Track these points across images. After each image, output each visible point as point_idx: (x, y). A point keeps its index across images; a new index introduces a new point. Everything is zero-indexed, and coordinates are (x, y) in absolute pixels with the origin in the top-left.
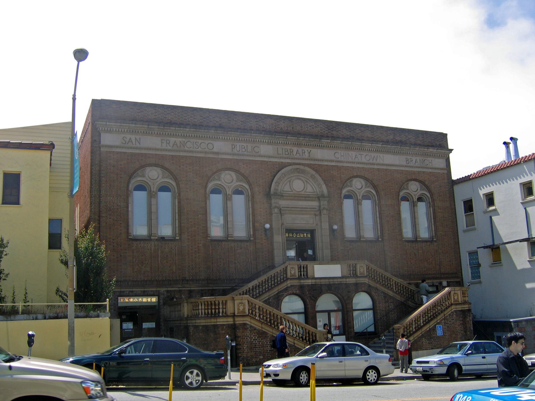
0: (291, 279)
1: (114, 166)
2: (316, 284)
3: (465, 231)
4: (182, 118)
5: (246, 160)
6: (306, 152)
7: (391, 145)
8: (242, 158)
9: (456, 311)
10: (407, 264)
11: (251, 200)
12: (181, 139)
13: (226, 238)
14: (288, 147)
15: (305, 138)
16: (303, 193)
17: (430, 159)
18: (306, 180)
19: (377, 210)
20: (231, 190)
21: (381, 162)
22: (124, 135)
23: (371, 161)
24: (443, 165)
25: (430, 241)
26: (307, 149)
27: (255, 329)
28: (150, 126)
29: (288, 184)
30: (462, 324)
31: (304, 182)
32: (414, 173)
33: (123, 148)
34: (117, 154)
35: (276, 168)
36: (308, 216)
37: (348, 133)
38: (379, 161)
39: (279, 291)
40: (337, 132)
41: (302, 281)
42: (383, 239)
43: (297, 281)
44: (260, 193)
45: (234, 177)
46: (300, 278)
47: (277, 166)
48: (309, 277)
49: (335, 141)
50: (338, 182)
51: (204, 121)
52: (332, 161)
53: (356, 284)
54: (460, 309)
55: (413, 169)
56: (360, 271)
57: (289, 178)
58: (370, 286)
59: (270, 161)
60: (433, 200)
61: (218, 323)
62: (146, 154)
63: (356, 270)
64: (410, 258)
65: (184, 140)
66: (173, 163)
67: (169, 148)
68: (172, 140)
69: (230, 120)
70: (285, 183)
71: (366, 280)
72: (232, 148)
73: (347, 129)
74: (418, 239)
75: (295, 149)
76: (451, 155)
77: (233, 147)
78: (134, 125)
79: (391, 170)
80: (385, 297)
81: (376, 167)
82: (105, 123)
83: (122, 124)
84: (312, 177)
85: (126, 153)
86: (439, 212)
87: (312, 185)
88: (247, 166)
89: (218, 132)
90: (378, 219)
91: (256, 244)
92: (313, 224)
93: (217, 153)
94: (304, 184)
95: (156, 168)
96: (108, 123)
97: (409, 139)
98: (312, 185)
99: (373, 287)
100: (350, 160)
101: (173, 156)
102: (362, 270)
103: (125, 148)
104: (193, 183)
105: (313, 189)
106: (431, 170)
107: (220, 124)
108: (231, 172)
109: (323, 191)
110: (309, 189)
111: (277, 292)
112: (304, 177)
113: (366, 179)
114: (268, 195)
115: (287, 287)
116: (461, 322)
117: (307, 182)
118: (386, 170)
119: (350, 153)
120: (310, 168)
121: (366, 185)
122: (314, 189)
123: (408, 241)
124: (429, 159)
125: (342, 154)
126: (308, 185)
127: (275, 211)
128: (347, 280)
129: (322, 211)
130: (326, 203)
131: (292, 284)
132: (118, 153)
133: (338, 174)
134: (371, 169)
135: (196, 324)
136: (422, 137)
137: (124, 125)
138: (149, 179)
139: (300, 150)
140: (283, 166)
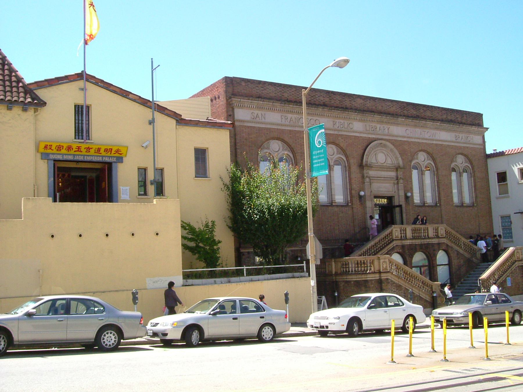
0: (396, 240)
1: (246, 139)
3: (497, 198)
4: (296, 96)
5: (344, 135)
8: (341, 133)
9: (518, 266)
11: (347, 170)
12: (295, 116)
13: (329, 203)
14: (373, 124)
15: (387, 116)
16: (385, 164)
17: (471, 136)
18: (387, 153)
19: (436, 179)
20: (333, 161)
21: (438, 138)
22: (252, 111)
23: (431, 138)
24: (480, 141)
25: (472, 206)
26: (387, 126)
27: (394, 283)
28: (274, 104)
29: (375, 156)
32: (460, 148)
33: (252, 122)
35: (365, 142)
36: (389, 185)
37: (415, 113)
39: (388, 250)
40: (407, 111)
41: (403, 242)
42: (440, 205)
43: (400, 242)
44: (355, 164)
45: (335, 150)
46: (401, 239)
47: (366, 141)
48: (407, 238)
49: (408, 120)
51: (312, 99)
52: (404, 137)
53: (439, 244)
54: (521, 265)
55: (460, 145)
57: (375, 152)
58: (447, 245)
60: (474, 172)
61: (368, 279)
62: (270, 129)
63: (437, 232)
65: (298, 116)
66: (291, 137)
67: (287, 123)
68: (289, 116)
69: (331, 99)
71: (444, 241)
73: (414, 109)
74: (464, 205)
75: (378, 126)
76: (487, 134)
77: (334, 123)
78: (262, 102)
80: (457, 254)
81: (434, 142)
82: (240, 100)
83: (253, 101)
84: (391, 150)
86: (478, 182)
87: (391, 157)
88: (344, 140)
89: (325, 110)
90: (436, 187)
91: (353, 209)
92: (392, 191)
94: (386, 157)
95: (277, 141)
96: (242, 100)
97: (457, 118)
98: (391, 157)
99: (450, 247)
100: (417, 136)
102: (442, 233)
103: (254, 122)
105: (392, 161)
106: (472, 146)
107: (324, 103)
108: (332, 145)
109: (399, 163)
110: (389, 161)
111: (387, 251)
112: (386, 151)
113: (428, 153)
114: (361, 166)
115: (393, 247)
117: (387, 155)
118: (442, 145)
120: (389, 142)
121: (428, 158)
122: (393, 161)
123: (457, 206)
124: (471, 136)
127: (367, 181)
128: (433, 240)
129: (399, 181)
130: (401, 173)
131: (397, 244)
132: (248, 127)
133: (409, 148)
135: (348, 280)
136: (466, 117)
137: (255, 101)
138: (273, 152)
139: (382, 126)
140: (370, 141)
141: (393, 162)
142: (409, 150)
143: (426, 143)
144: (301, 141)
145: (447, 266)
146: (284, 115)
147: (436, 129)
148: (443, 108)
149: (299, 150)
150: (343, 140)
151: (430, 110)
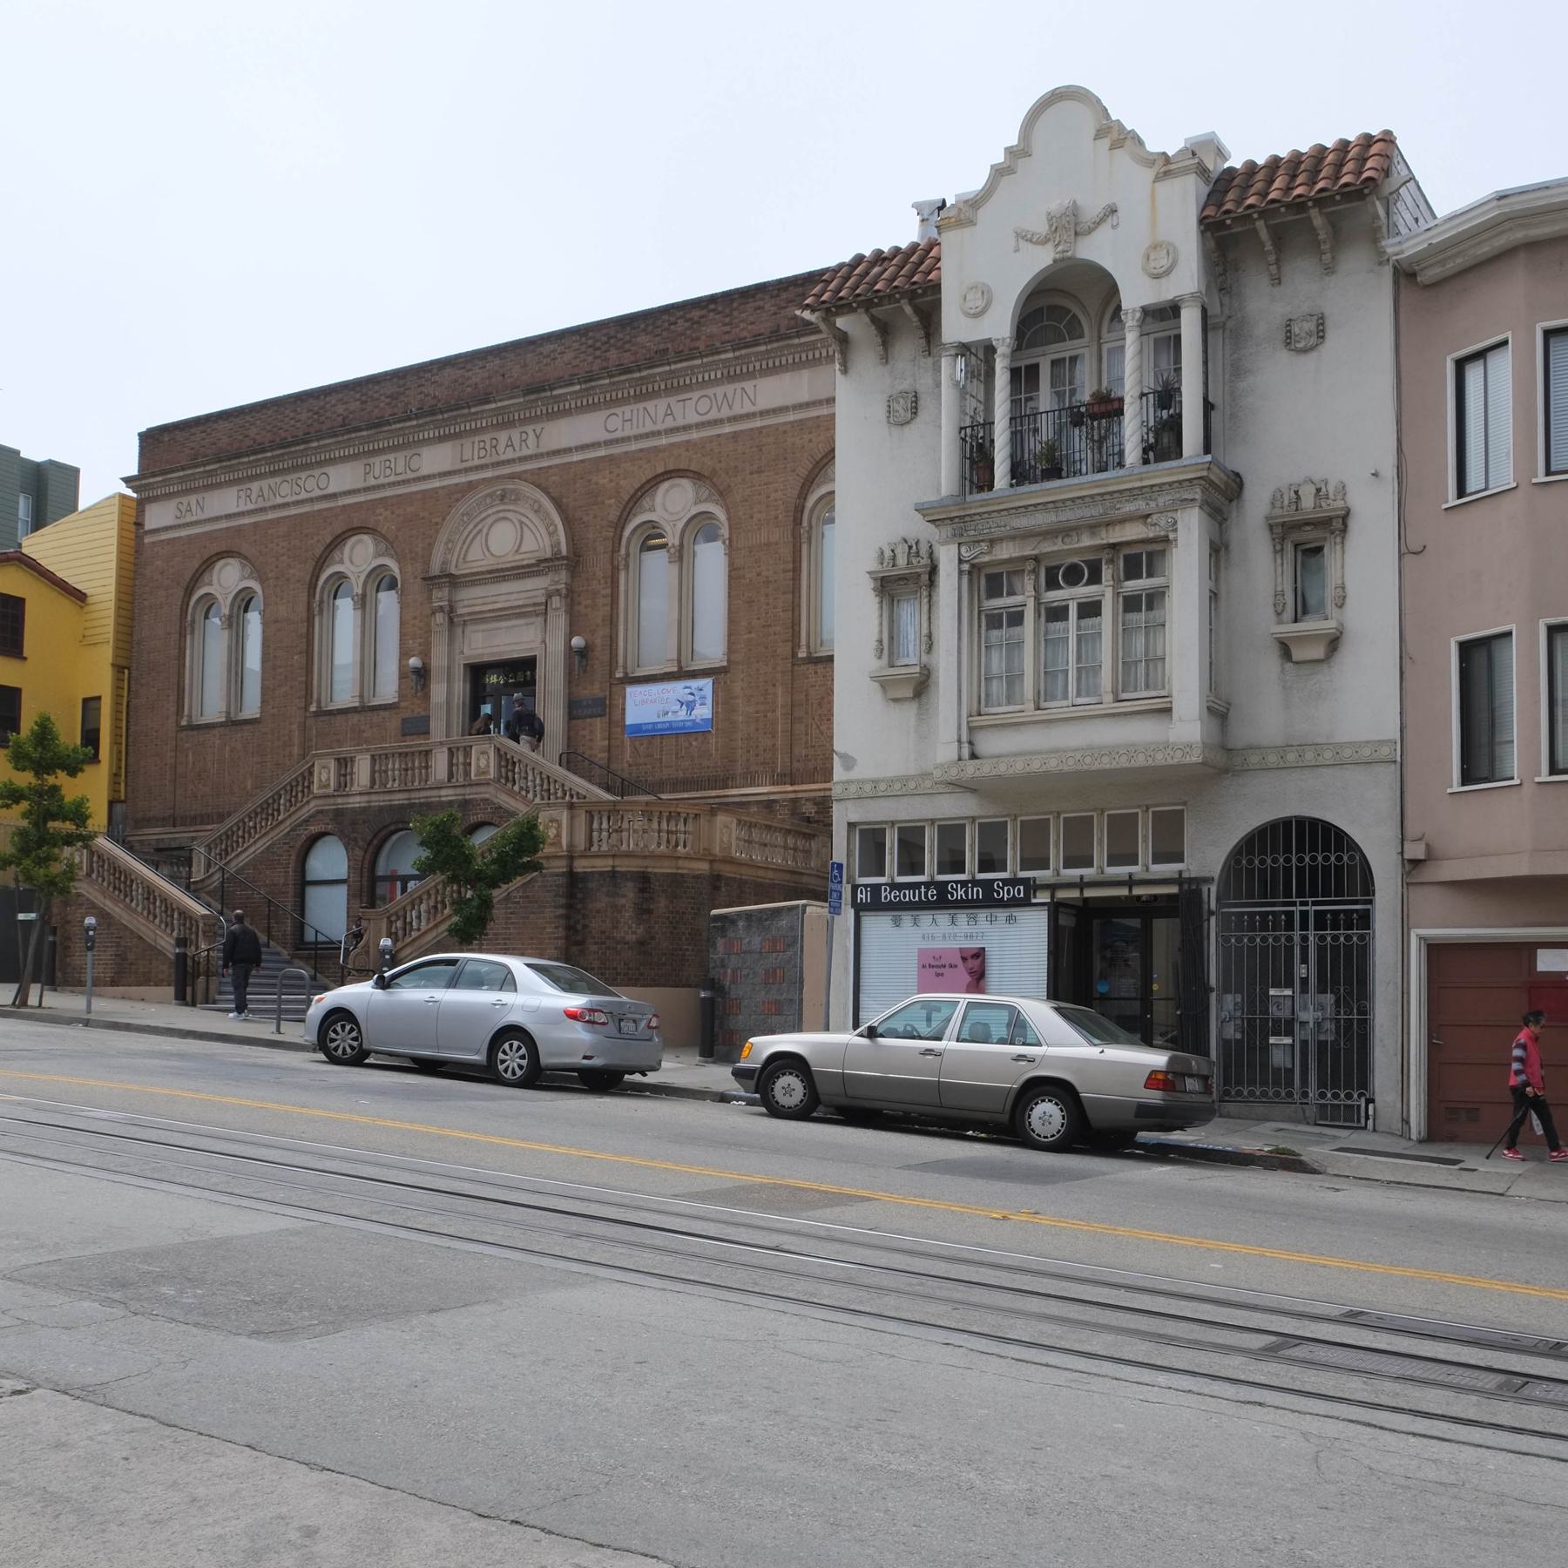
2: (370, 807)
6: (531, 434)
7: (765, 343)
10: (807, 734)
18: (520, 517)
21: (748, 408)
26: (532, 427)
30: (560, 916)
31: (487, 534)
34: (168, 544)
38: (764, 403)
50: (610, 506)
56: (478, 766)
59: (443, 487)
64: (820, 715)
67: (250, 507)
70: (471, 537)
72: (366, 474)
79: (776, 427)
85: (180, 538)
93: (334, 496)
100: (649, 427)
101: (256, 524)
104: (288, 580)
110: (530, 544)
116: (562, 911)
117: (521, 523)
118: (760, 430)
119: (650, 405)
122: (540, 540)
125: (627, 416)
126: (525, 528)
133: (611, 481)
134: (711, 439)
141: (542, 545)
142: (613, 484)
143: (688, 441)
144: (278, 545)
145: (309, 878)
146: (244, 487)
147: (732, 378)
148: (780, 281)
149: (271, 571)
150: (388, 513)
151: (720, 308)
